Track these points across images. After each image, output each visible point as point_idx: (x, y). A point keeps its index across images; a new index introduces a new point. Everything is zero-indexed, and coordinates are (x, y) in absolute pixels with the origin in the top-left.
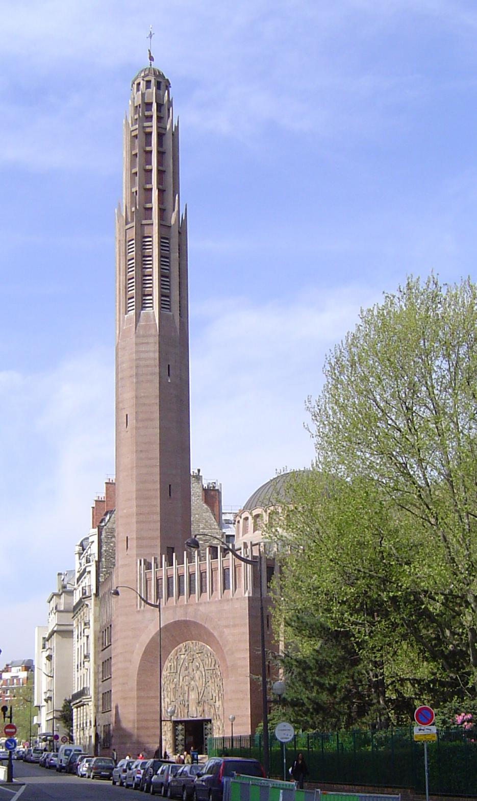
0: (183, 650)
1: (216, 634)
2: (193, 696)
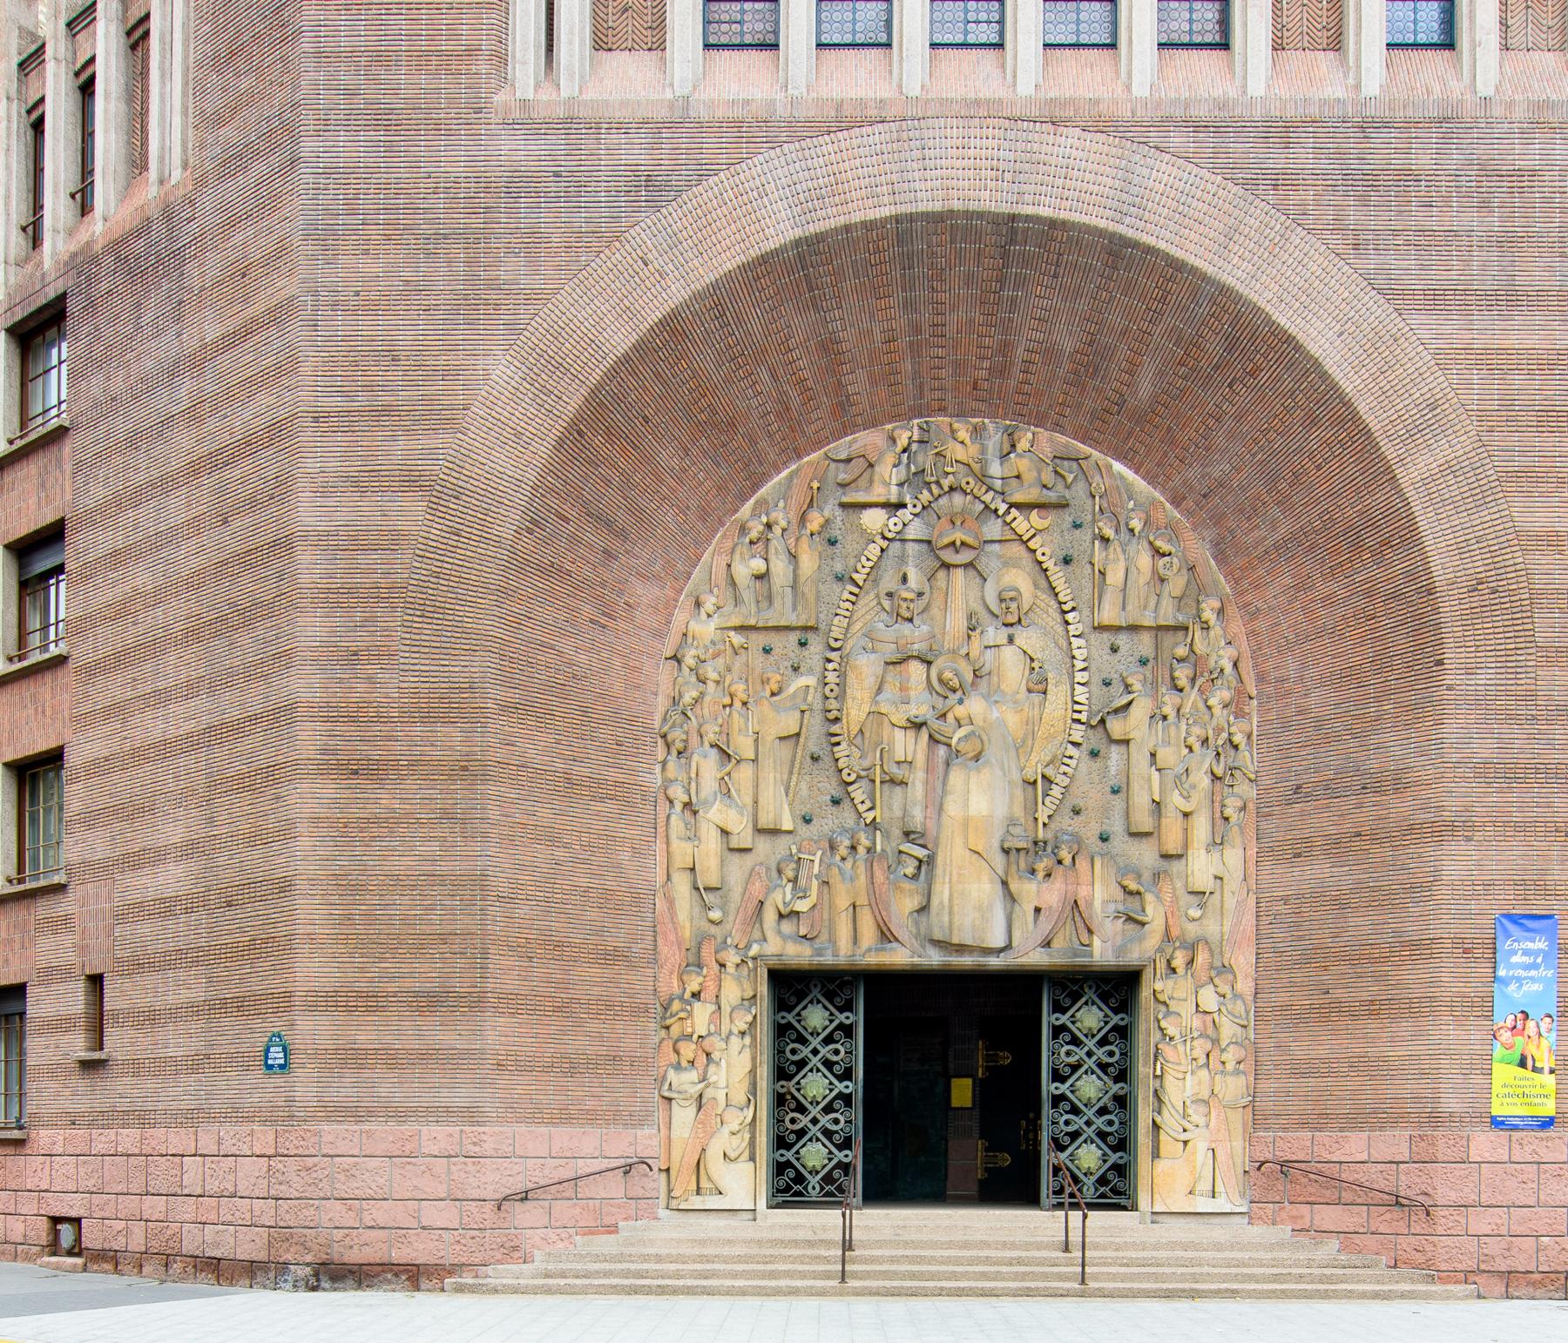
0: (888, 479)
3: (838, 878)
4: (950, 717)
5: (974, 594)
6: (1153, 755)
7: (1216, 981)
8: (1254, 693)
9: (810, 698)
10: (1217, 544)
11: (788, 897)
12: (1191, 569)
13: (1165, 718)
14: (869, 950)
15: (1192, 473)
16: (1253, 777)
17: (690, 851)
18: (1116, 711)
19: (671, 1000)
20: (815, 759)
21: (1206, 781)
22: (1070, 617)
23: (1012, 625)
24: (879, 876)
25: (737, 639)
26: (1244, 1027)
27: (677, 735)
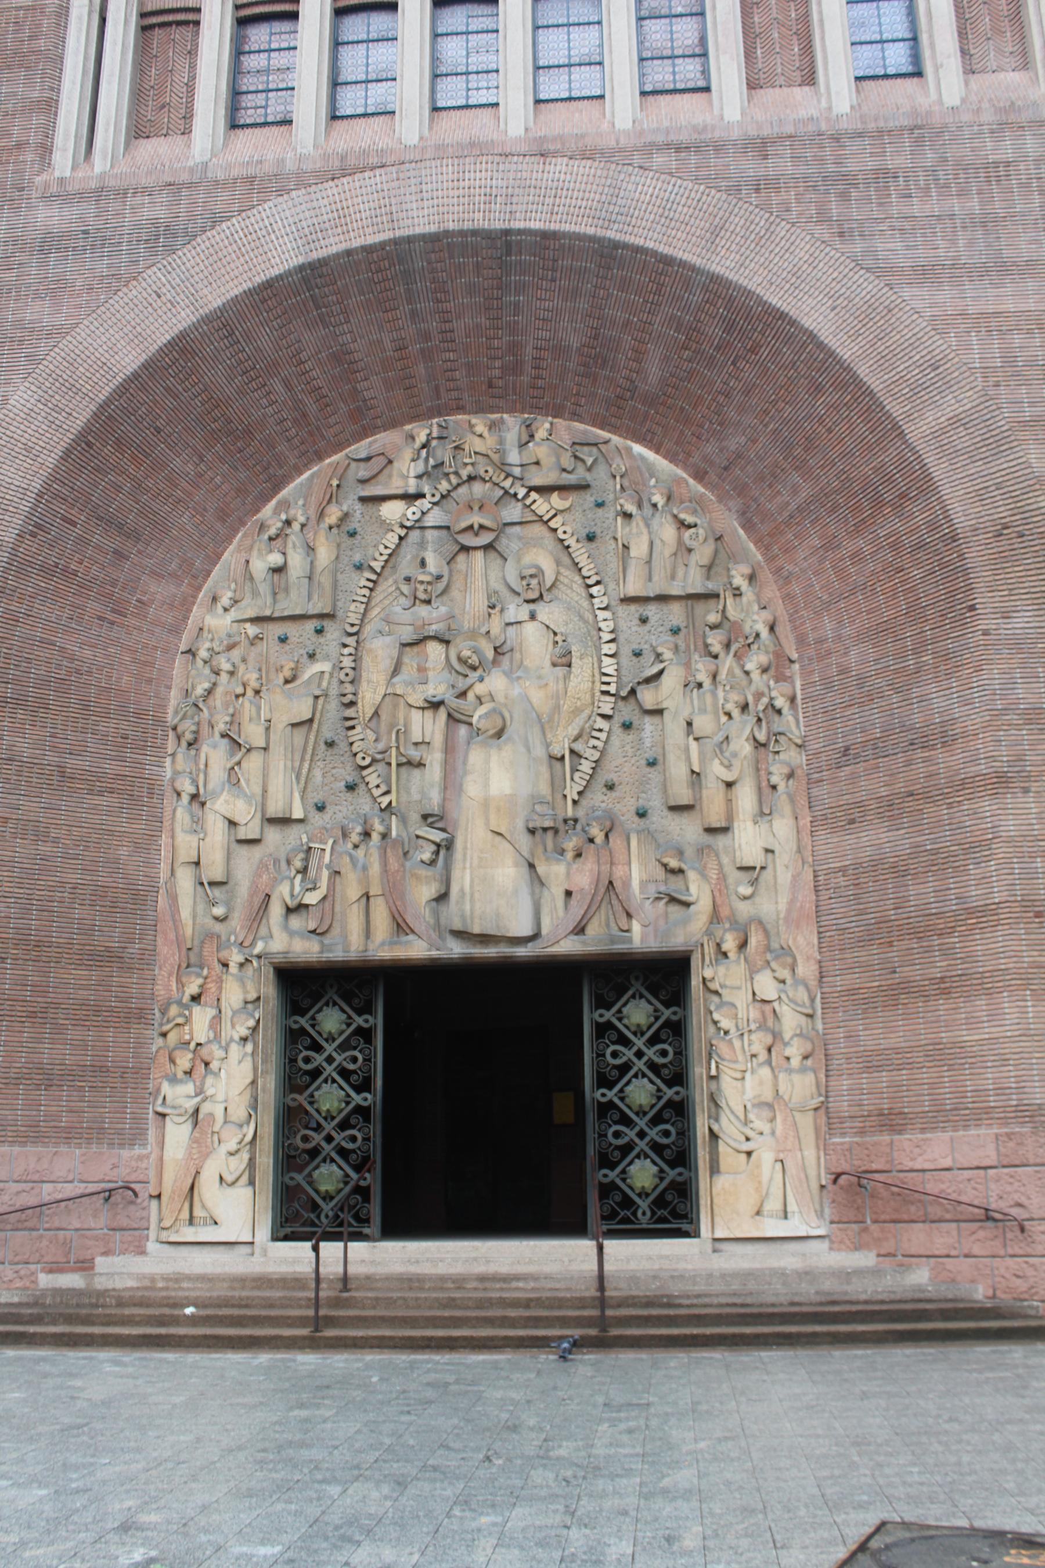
0: (406, 472)
1: (814, 316)
2: (498, 781)
3: (349, 866)
4: (471, 695)
5: (494, 575)
6: (689, 724)
7: (773, 965)
8: (795, 656)
9: (324, 684)
10: (744, 513)
11: (297, 889)
12: (719, 539)
13: (700, 685)
14: (383, 944)
15: (710, 448)
16: (799, 741)
17: (195, 845)
18: (648, 681)
19: (169, 1004)
20: (330, 744)
21: (748, 748)
22: (594, 590)
23: (533, 601)
24: (394, 864)
25: (252, 630)
26: (810, 1016)
27: (187, 727)
